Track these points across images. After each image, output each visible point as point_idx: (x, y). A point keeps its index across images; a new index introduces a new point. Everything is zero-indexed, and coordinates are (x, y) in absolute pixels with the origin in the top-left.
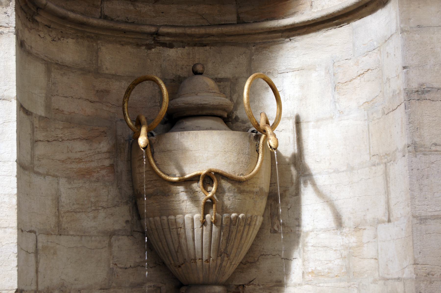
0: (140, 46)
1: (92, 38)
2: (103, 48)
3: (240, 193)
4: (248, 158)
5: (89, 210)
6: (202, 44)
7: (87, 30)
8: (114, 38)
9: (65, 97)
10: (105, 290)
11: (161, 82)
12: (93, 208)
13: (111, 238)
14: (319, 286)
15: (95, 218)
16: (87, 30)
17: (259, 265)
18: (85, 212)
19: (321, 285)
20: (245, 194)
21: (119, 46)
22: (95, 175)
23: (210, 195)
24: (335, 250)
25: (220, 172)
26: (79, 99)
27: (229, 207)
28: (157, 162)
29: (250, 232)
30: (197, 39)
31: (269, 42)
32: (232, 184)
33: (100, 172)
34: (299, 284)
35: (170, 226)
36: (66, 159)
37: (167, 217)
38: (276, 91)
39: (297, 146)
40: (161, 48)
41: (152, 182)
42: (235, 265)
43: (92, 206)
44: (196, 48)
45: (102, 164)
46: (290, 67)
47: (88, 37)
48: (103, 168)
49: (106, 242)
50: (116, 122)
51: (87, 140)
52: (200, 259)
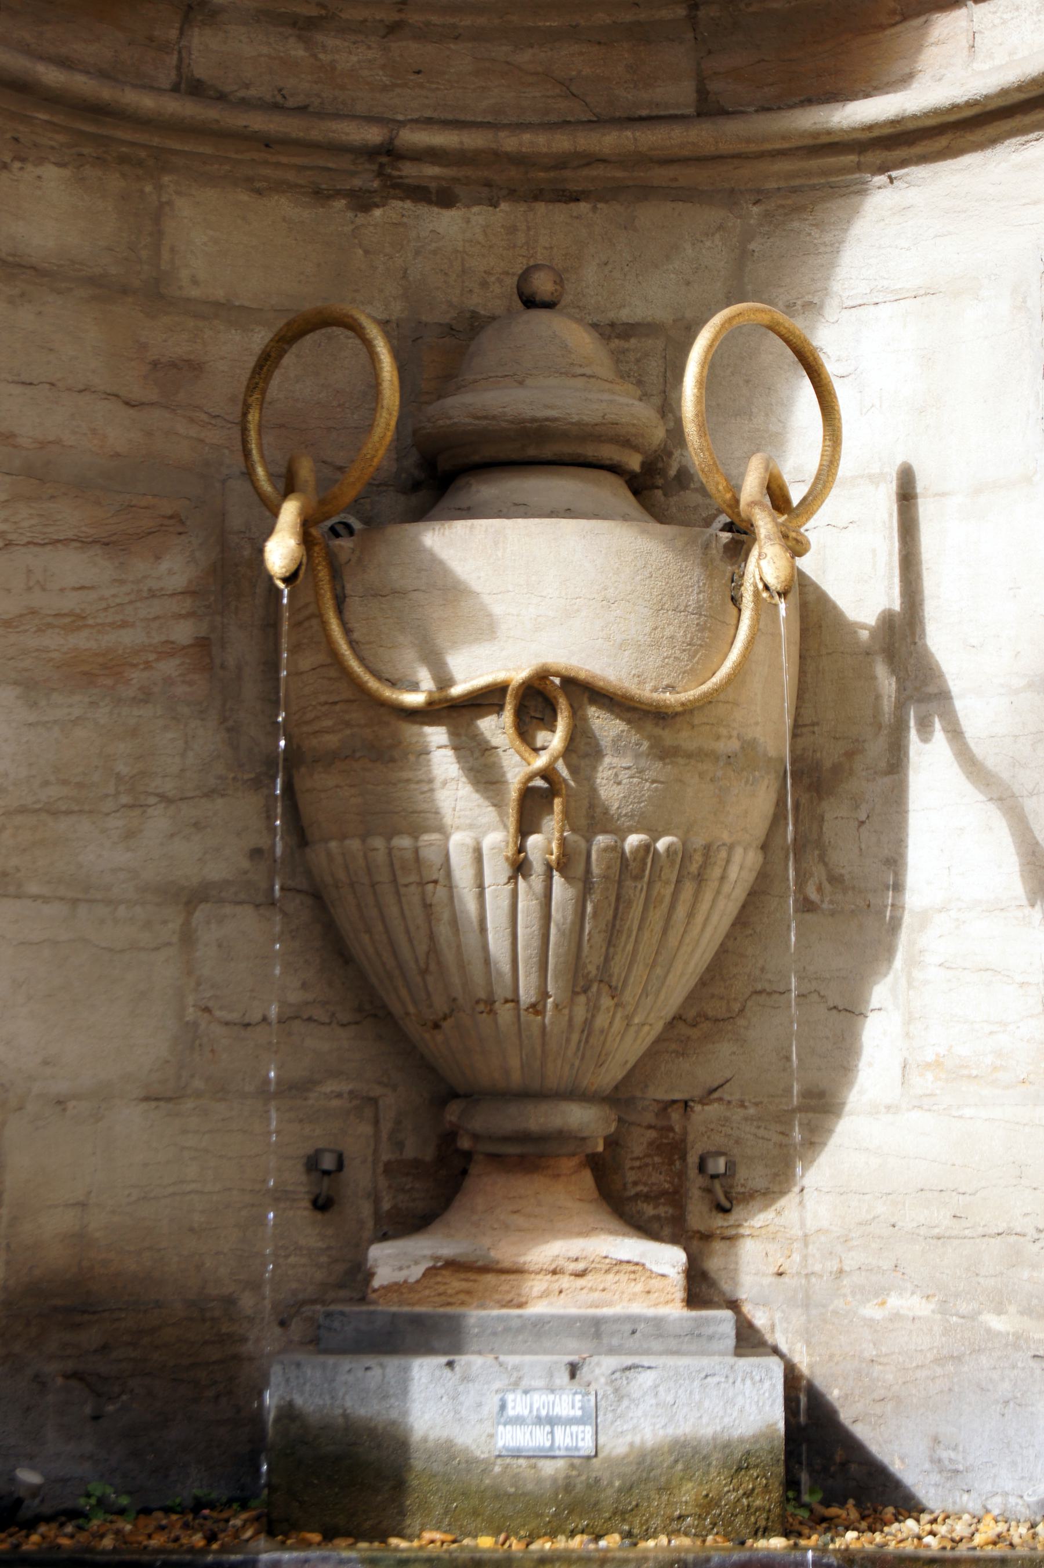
0: (329, 197)
1: (140, 163)
2: (180, 202)
3: (661, 758)
4: (698, 624)
5: (109, 805)
6: (564, 191)
7: (119, 134)
8: (227, 167)
9: (23, 383)
10: (162, 1104)
11: (374, 332)
12: (124, 799)
13: (190, 914)
14: (961, 1117)
15: (129, 835)
16: (119, 134)
17: (747, 1028)
18: (91, 812)
19: (968, 1112)
20: (681, 761)
21: (244, 197)
22: (137, 676)
23: (541, 761)
24: (1022, 985)
25: (582, 675)
26: (80, 391)
27: (618, 808)
28: (356, 636)
29: (704, 907)
30: (542, 174)
31: (813, 188)
32: (629, 722)
33: (154, 665)
34: (888, 1108)
35: (399, 873)
36: (21, 616)
37: (389, 839)
38: (819, 375)
39: (901, 587)
40: (408, 204)
41: (338, 708)
42: (646, 1028)
43: (118, 793)
44: (541, 207)
45: (164, 638)
47: (123, 159)
48: (169, 650)
49: (170, 925)
50: (224, 482)
51: (107, 544)
52: (506, 1001)
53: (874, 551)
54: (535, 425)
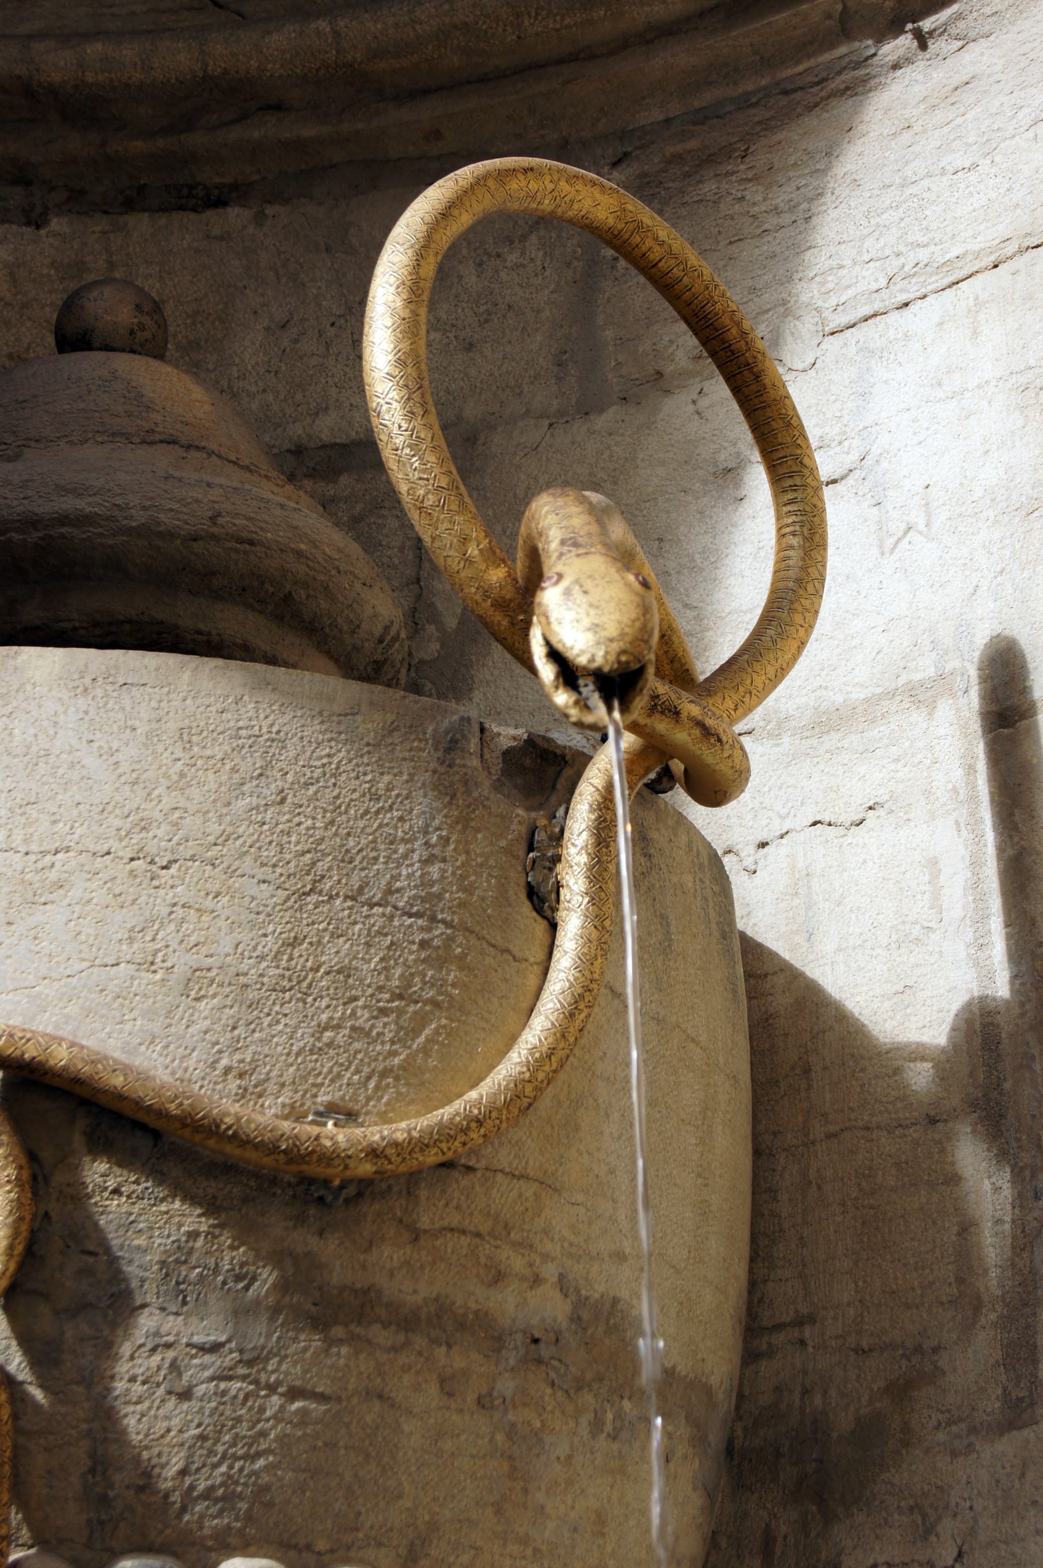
3: (318, 1323)
4: (424, 944)
6: (191, 187)
20: (381, 1335)
25: (60, 1057)
27: (183, 1472)
30: (138, 146)
31: (745, 103)
32: (211, 1207)
38: (757, 377)
39: (1009, 937)
44: (141, 224)
46: (923, 255)
53: (933, 864)
54: (34, 536)
